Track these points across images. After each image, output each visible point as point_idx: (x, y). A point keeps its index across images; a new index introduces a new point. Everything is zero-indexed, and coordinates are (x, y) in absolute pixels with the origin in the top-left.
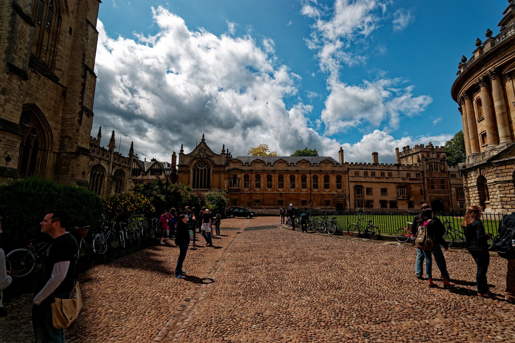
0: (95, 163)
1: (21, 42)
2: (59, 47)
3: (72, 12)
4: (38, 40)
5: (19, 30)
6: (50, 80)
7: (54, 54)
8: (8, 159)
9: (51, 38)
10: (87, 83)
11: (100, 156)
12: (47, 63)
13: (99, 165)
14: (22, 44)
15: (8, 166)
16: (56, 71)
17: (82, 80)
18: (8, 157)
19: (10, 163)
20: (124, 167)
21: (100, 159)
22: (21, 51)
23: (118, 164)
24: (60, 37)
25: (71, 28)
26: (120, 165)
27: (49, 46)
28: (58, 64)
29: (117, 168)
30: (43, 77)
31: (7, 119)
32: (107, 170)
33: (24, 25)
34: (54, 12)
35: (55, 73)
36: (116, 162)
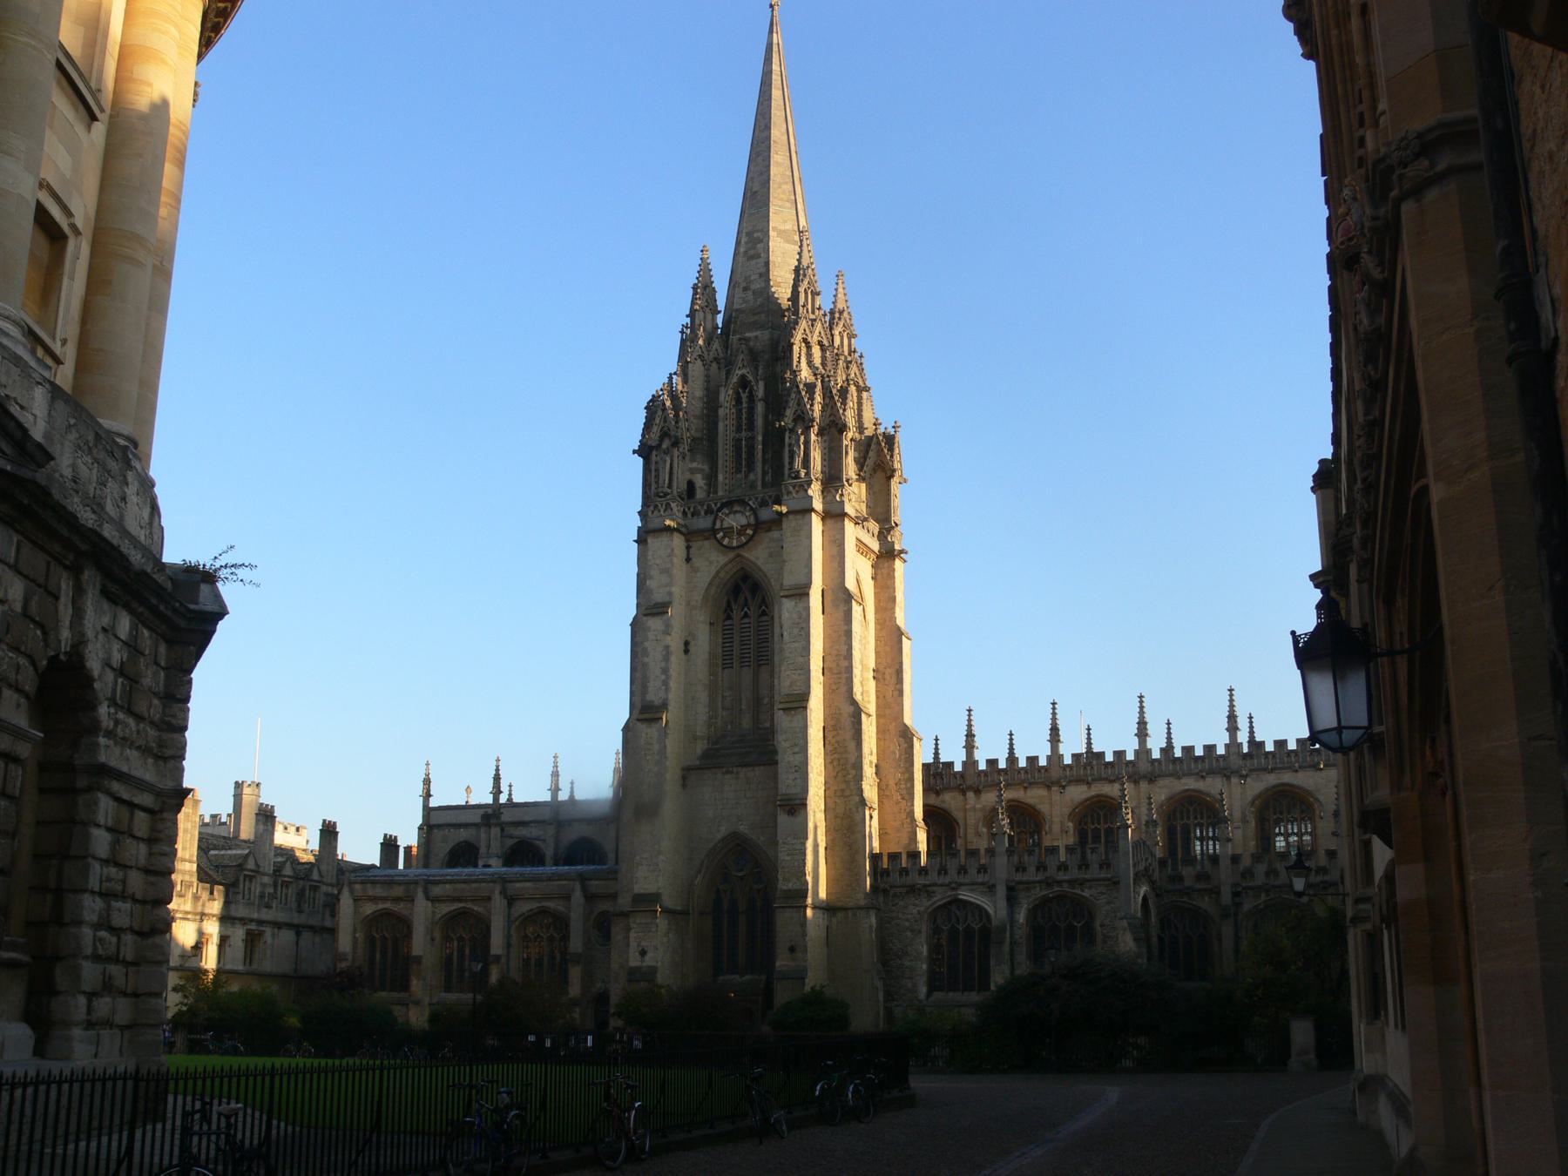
0: (935, 902)
6: (756, 768)
8: (643, 953)
13: (957, 901)
15: (644, 964)
18: (643, 950)
19: (647, 958)
20: (1082, 883)
23: (1039, 882)
26: (1048, 883)
29: (1039, 892)
30: (744, 770)
31: (642, 891)
32: (991, 911)
33: (649, 730)
36: (1031, 875)
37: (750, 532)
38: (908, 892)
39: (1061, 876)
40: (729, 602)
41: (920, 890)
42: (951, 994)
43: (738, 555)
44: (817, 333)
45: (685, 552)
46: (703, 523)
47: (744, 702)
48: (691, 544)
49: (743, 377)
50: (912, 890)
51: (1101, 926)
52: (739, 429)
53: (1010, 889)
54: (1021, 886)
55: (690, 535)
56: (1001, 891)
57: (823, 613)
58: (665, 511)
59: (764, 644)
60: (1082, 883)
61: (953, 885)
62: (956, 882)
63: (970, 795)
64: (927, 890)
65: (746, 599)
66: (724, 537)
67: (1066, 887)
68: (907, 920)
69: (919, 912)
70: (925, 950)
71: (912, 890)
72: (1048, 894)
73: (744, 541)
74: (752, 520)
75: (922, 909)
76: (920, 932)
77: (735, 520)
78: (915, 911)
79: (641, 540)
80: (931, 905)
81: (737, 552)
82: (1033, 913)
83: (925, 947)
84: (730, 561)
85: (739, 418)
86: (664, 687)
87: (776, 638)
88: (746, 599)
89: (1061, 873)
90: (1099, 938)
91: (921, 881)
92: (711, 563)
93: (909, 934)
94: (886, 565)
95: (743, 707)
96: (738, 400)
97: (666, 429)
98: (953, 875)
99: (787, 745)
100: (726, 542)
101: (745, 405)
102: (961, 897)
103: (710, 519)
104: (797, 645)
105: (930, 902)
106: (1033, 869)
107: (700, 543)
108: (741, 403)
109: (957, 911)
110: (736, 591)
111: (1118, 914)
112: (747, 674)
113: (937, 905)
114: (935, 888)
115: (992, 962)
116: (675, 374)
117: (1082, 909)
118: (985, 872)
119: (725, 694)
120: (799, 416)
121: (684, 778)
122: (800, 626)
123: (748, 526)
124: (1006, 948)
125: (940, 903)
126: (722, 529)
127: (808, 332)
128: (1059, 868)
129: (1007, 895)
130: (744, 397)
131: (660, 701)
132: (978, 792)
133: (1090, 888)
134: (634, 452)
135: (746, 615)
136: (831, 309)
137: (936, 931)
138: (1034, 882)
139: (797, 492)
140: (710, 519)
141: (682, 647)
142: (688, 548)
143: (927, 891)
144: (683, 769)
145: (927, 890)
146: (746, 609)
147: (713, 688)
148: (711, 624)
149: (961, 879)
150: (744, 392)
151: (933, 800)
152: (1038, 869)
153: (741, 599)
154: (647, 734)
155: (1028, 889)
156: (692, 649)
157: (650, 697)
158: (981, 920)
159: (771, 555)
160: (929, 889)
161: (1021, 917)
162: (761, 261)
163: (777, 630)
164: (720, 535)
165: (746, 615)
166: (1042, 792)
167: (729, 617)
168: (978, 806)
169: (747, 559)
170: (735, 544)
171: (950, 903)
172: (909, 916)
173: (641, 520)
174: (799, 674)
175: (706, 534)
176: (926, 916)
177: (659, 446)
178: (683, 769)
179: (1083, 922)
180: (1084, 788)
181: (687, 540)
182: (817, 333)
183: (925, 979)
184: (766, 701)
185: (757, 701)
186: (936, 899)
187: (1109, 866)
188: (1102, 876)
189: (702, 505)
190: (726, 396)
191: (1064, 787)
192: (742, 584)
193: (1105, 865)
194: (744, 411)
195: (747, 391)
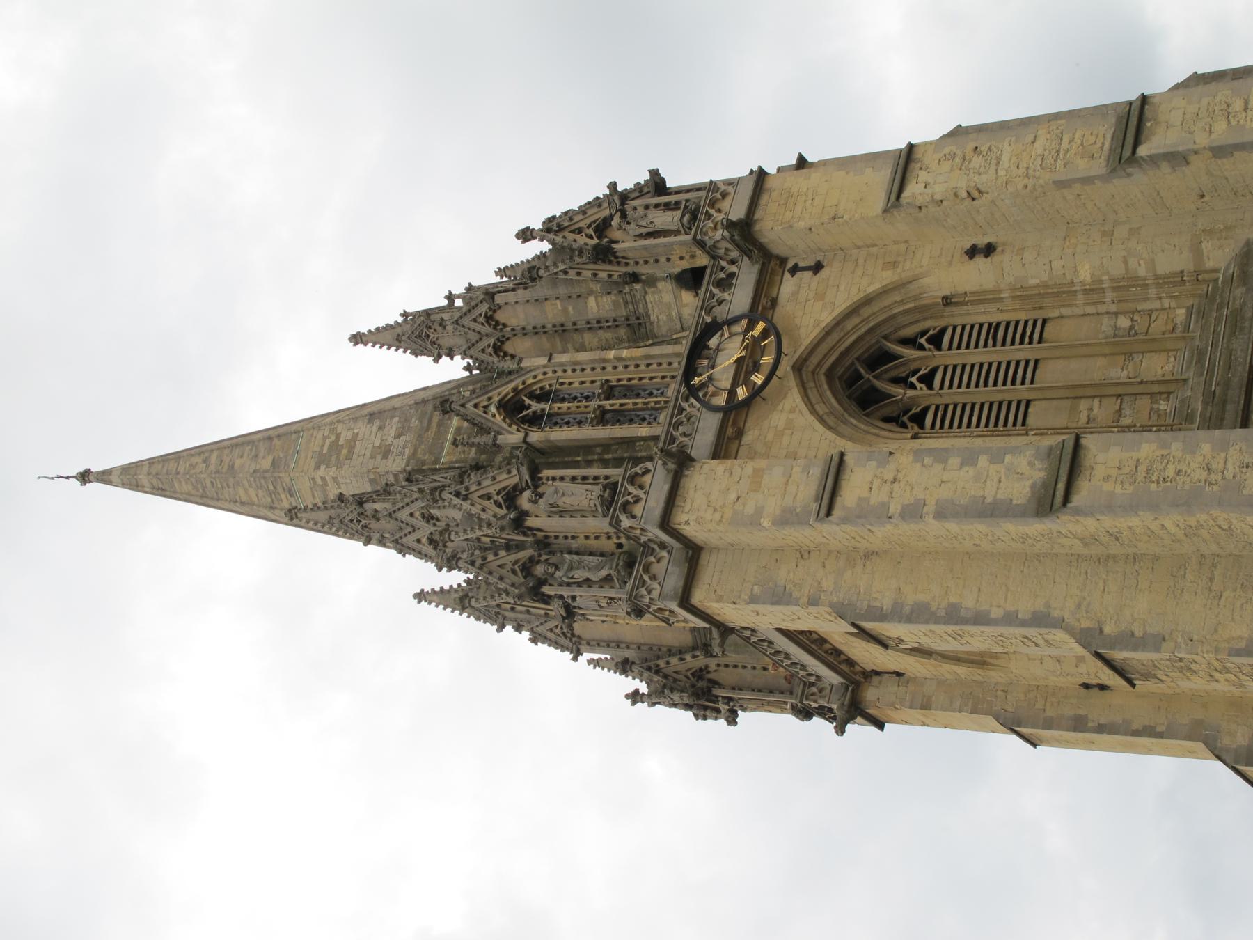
1: (1178, 472)
2: (1085, 274)
3: (894, 264)
4: (1105, 355)
5: (1130, 489)
7: (1127, 285)
9: (1065, 311)
10: (1202, 140)
12: (1189, 302)
14: (1183, 467)
16: (1210, 264)
17: (1197, 163)
22: (1217, 465)
24: (1033, 282)
25: (972, 252)
27: (1102, 309)
28: (1174, 260)
33: (1100, 472)
34: (941, 323)
35: (1223, 265)
49: (503, 406)
58: (641, 487)
65: (897, 381)
81: (785, 366)
86: (1008, 458)
92: (790, 425)
99: (1220, 126)
100: (758, 379)
104: (1005, 158)
122: (969, 154)
130: (536, 406)
131: (1038, 465)
154: (1107, 478)
157: (1020, 491)
159: (820, 297)
162: (362, 428)
165: (928, 380)
174: (1071, 141)
195: (527, 401)
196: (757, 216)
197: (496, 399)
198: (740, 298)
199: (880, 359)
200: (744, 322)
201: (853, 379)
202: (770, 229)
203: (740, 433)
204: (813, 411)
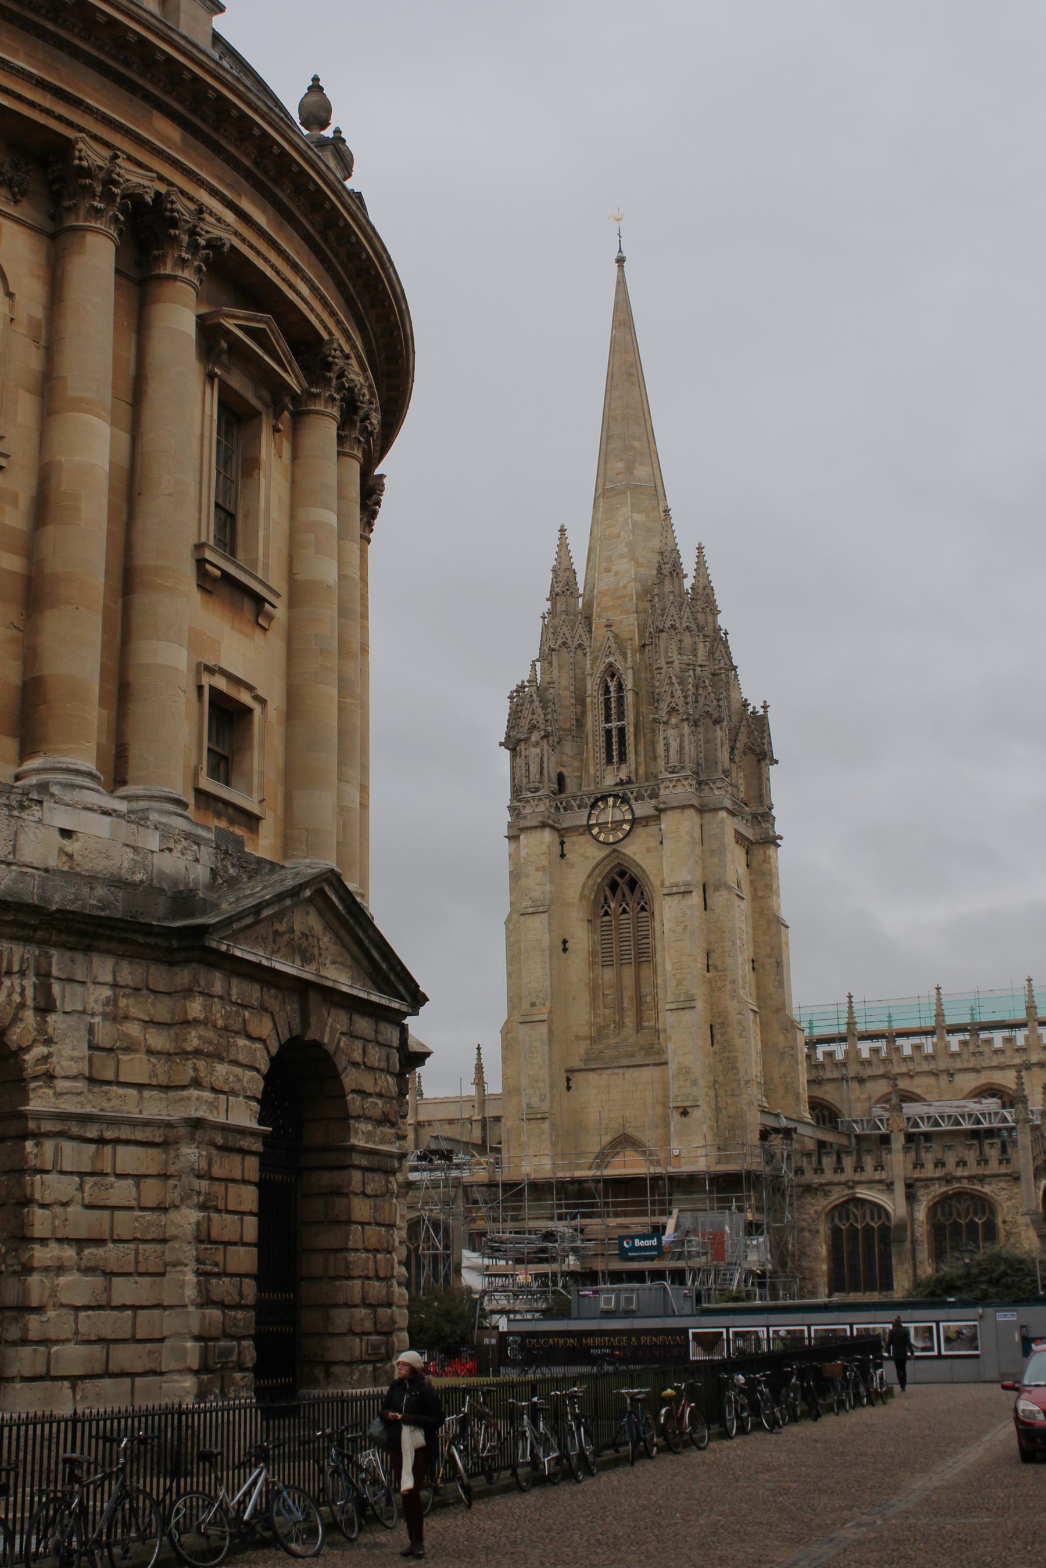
11: (849, 1174)
20: (982, 1179)
21: (852, 1185)
23: (939, 1179)
26: (948, 1179)
29: (938, 1190)
30: (631, 1070)
36: (929, 1171)
37: (626, 827)
38: (804, 1192)
39: (960, 1172)
40: (606, 898)
41: (816, 1189)
42: (852, 1294)
43: (615, 851)
44: (685, 618)
45: (558, 847)
46: (580, 818)
47: (626, 1001)
48: (565, 839)
49: (611, 665)
50: (809, 1189)
51: (1004, 1222)
52: (608, 719)
53: (909, 1186)
54: (919, 1184)
55: (562, 834)
56: (900, 1189)
57: (706, 909)
59: (645, 941)
60: (982, 1179)
61: (850, 1184)
62: (853, 1181)
63: (855, 1085)
64: (823, 1189)
66: (599, 833)
67: (965, 1184)
68: (804, 1220)
69: (816, 1211)
70: (824, 1251)
71: (809, 1189)
72: (946, 1192)
73: (621, 836)
74: (630, 817)
75: (819, 1208)
76: (818, 1232)
77: (610, 813)
78: (812, 1211)
79: (513, 838)
80: (829, 1204)
81: (614, 846)
82: (932, 1210)
83: (824, 1247)
84: (607, 857)
85: (608, 708)
87: (658, 934)
88: (624, 895)
89: (960, 1169)
90: (1002, 1234)
91: (817, 1180)
92: (587, 858)
93: (806, 1234)
94: (761, 851)
95: (625, 1005)
96: (607, 690)
97: (534, 721)
98: (849, 1174)
100: (602, 838)
101: (612, 694)
102: (858, 1195)
103: (585, 812)
105: (826, 1202)
106: (930, 1166)
107: (575, 839)
108: (610, 692)
109: (855, 1210)
110: (614, 886)
111: (1020, 1210)
112: (628, 972)
113: (833, 1205)
114: (830, 1187)
115: (894, 1261)
116: (538, 660)
117: (984, 1205)
118: (883, 1169)
119: (606, 992)
120: (673, 708)
121: (568, 1080)
123: (624, 821)
124: (908, 1245)
125: (838, 1202)
126: (597, 825)
127: (676, 617)
128: (958, 1164)
129: (906, 1193)
132: (861, 1081)
133: (990, 1184)
134: (501, 744)
135: (624, 911)
136: (693, 585)
137: (836, 1232)
138: (932, 1179)
139: (674, 786)
140: (585, 812)
141: (562, 946)
142: (562, 843)
143: (824, 1190)
144: (567, 1071)
145: (823, 1189)
146: (624, 905)
147: (594, 989)
148: (589, 921)
149: (857, 1177)
150: (612, 681)
151: (818, 1092)
152: (936, 1165)
153: (619, 893)
155: (926, 1187)
156: (568, 946)
158: (880, 1218)
159: (648, 850)
160: (826, 1188)
161: (921, 1214)
163: (657, 924)
164: (595, 831)
166: (931, 1080)
167: (606, 914)
168: (863, 1096)
169: (625, 855)
170: (611, 840)
171: (847, 1202)
172: (806, 1217)
173: (511, 816)
175: (581, 830)
176: (823, 1216)
177: (526, 740)
178: (570, 1071)
179: (984, 1219)
180: (971, 1076)
181: (561, 836)
182: (685, 618)
183: (825, 1279)
184: (648, 999)
185: (639, 1000)
186: (833, 1198)
187: (1008, 1161)
188: (1002, 1171)
189: (575, 800)
190: (592, 686)
191: (951, 1075)
192: (618, 879)
193: (1004, 1160)
194: (612, 700)
196: (669, 812)
197: (611, 659)
198: (642, 809)
199: (633, 884)
200: (630, 817)
201: (622, 874)
202: (668, 821)
203: (581, 834)
204: (594, 869)
